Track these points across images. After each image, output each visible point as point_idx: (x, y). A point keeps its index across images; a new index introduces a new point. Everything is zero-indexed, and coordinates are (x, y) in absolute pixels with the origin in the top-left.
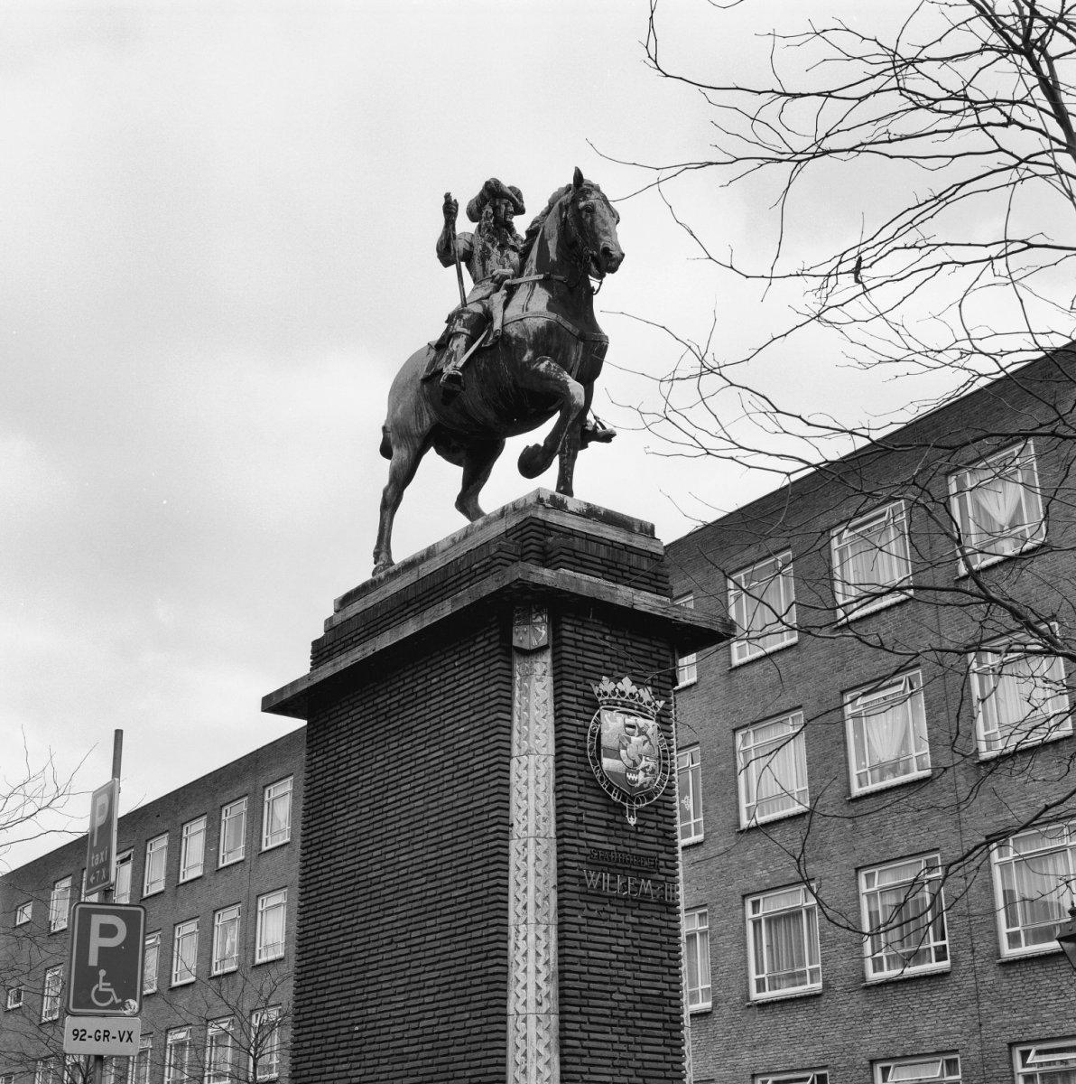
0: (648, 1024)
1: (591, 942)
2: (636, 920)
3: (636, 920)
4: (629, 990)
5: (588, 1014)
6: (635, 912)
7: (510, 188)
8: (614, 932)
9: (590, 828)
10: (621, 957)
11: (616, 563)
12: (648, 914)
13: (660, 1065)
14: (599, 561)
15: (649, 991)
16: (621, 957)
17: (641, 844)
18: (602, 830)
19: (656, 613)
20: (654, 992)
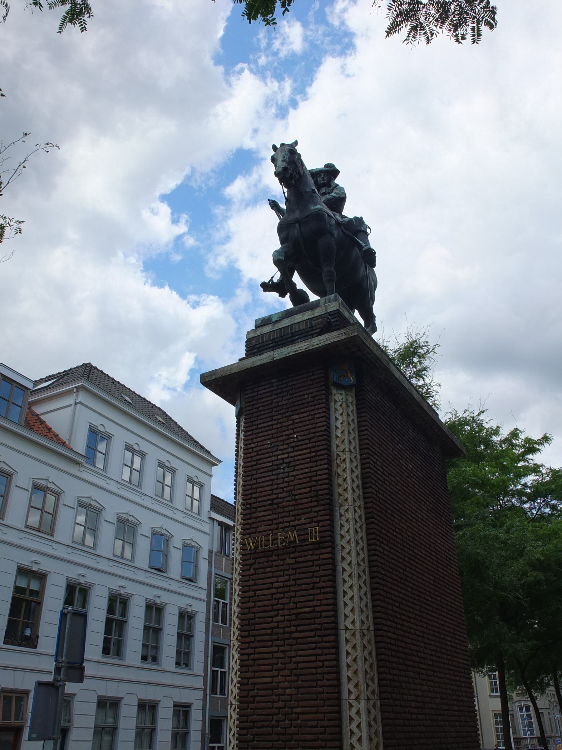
0: (302, 634)
1: (258, 585)
2: (293, 561)
3: (293, 561)
4: (286, 612)
5: (254, 636)
6: (292, 556)
7: (325, 167)
8: (275, 574)
10: (280, 590)
11: (282, 337)
12: (302, 554)
13: (312, 664)
14: (270, 342)
15: (303, 610)
16: (280, 590)
18: (267, 508)
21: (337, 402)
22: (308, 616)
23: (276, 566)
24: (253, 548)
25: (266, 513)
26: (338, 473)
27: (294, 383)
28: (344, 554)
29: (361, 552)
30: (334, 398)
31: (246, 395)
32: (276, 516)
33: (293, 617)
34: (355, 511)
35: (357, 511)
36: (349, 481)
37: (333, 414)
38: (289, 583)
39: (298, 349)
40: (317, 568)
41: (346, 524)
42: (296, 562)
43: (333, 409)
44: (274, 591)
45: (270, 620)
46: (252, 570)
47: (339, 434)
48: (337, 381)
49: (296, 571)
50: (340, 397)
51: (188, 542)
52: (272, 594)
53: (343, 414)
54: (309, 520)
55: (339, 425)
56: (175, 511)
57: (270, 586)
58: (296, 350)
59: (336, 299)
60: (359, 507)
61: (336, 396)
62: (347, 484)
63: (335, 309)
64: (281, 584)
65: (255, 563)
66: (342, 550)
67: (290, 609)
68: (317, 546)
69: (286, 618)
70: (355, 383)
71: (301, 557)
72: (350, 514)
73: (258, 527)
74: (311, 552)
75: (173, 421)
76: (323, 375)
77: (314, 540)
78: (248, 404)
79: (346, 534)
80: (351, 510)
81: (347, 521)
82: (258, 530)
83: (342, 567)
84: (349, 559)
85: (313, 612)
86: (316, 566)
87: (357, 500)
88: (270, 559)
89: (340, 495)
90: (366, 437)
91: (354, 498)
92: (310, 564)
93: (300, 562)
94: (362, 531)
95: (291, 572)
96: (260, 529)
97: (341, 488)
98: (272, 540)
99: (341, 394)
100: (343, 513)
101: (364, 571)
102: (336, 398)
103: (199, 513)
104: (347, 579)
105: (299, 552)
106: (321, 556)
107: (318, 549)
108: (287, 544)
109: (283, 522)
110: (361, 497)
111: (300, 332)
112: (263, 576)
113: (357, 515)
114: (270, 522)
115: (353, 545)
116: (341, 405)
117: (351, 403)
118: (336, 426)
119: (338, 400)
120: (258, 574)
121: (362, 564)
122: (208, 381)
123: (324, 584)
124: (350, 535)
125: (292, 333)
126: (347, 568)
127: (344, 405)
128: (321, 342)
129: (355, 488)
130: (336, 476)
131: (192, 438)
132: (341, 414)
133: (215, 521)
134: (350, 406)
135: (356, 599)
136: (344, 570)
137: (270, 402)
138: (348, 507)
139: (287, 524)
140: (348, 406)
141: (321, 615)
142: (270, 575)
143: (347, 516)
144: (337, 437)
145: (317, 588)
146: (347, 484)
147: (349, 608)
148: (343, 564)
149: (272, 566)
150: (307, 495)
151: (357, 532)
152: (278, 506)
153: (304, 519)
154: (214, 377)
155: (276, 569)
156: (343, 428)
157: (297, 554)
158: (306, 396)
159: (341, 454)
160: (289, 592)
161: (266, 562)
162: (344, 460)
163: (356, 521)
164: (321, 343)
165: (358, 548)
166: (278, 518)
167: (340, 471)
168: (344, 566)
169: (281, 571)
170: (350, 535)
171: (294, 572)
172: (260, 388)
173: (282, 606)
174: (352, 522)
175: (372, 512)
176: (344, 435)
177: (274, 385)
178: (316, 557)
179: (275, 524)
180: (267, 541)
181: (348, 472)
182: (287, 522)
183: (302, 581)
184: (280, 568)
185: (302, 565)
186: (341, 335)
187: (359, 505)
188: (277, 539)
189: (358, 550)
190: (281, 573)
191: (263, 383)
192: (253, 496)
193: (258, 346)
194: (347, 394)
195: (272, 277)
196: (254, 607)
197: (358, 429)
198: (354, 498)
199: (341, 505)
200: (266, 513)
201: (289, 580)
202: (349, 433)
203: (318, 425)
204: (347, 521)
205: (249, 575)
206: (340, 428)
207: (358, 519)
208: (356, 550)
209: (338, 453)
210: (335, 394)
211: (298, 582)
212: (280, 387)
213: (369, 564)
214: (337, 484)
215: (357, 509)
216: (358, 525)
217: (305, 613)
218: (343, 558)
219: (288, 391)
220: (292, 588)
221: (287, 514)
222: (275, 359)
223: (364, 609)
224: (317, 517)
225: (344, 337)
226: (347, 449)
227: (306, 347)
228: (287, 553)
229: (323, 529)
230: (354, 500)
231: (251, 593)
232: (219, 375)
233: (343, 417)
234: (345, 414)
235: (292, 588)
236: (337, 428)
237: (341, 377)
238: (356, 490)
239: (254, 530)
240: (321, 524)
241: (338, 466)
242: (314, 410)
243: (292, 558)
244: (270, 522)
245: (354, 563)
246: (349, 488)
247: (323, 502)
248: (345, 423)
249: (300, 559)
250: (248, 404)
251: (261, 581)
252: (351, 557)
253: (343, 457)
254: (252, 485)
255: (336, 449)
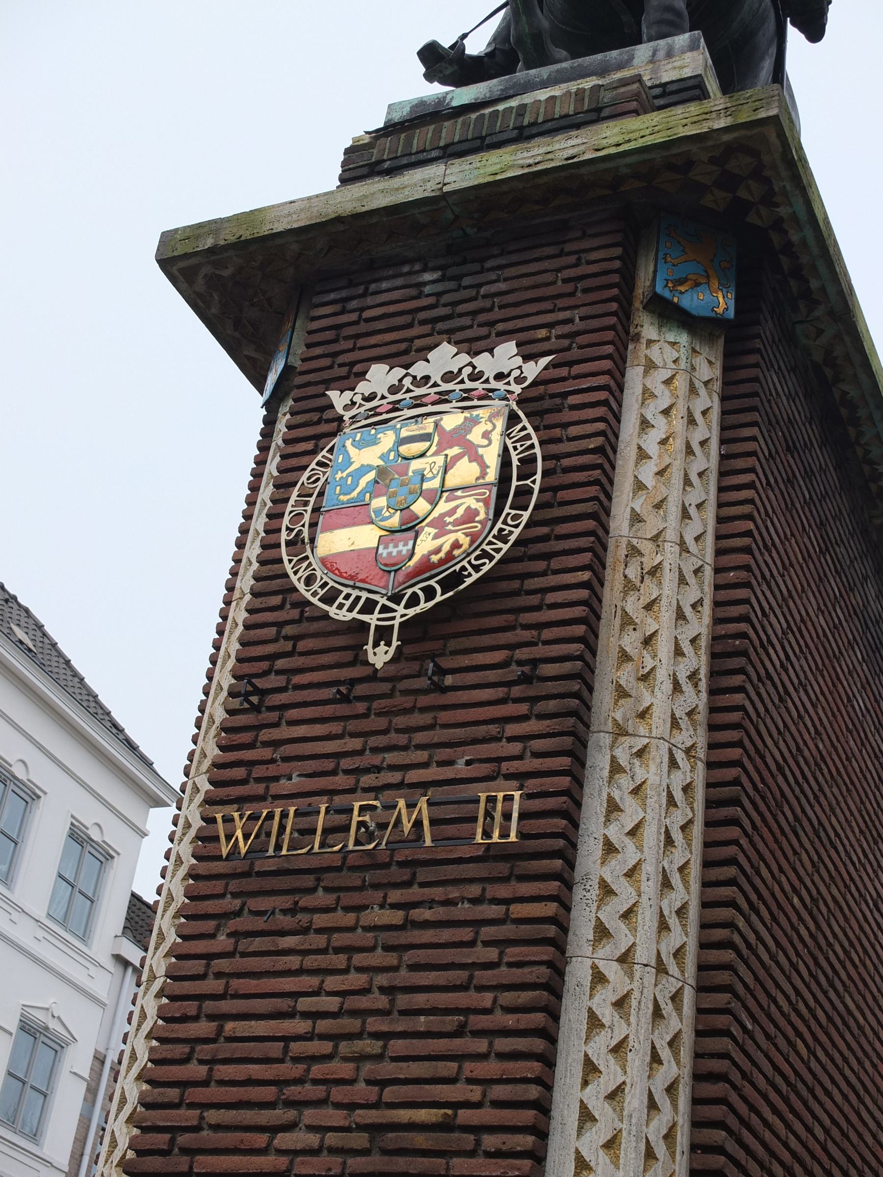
1: (236, 996)
2: (397, 917)
3: (397, 917)
4: (335, 1117)
6: (395, 896)
8: (311, 961)
9: (293, 714)
10: (323, 1025)
11: (483, 138)
12: (437, 893)
15: (405, 1115)
16: (323, 1025)
17: (445, 717)
19: (510, 174)
20: (423, 1115)
21: (655, 367)
22: (420, 1140)
23: (320, 931)
24: (243, 849)
25: (318, 730)
26: (625, 613)
27: (502, 286)
28: (610, 915)
29: (673, 921)
30: (648, 352)
31: (314, 319)
32: (355, 744)
33: (360, 1140)
34: (673, 764)
35: (679, 760)
36: (664, 647)
37: (636, 406)
38: (363, 1002)
39: (539, 159)
40: (492, 954)
41: (630, 804)
42: (409, 924)
43: (639, 390)
44: (300, 1026)
45: (261, 1139)
46: (222, 937)
47: (647, 476)
48: (667, 294)
49: (400, 958)
50: (670, 354)
51: (41, 1016)
52: (286, 1039)
53: (674, 412)
54: (484, 769)
55: (651, 446)
56: (15, 916)
57: (283, 1004)
58: (531, 161)
59: (693, 47)
60: (689, 751)
61: (656, 348)
62: (654, 656)
63: (687, 73)
64: (331, 1003)
65: (238, 913)
66: (601, 901)
67: (352, 1107)
68: (503, 868)
69: (332, 1139)
70: (731, 314)
71: (431, 903)
72: (653, 768)
73: (276, 779)
74: (475, 890)
75: (60, 654)
76: (617, 264)
77: (496, 838)
78: (318, 351)
79: (627, 840)
80: (659, 754)
81: (636, 791)
82: (275, 788)
83: (594, 967)
84: (623, 938)
85: (445, 1126)
86: (486, 944)
87: (683, 726)
88: (305, 901)
89: (622, 693)
90: (747, 509)
91: (673, 715)
92: (466, 934)
93: (426, 924)
94: (689, 845)
95: (379, 958)
96: (284, 786)
97: (629, 667)
98: (325, 831)
99: (673, 344)
100: (623, 761)
101: (676, 997)
102: (654, 353)
103: (85, 937)
104: (606, 1014)
105: (422, 885)
106: (512, 907)
107: (505, 880)
108: (383, 846)
109: (378, 769)
110: (702, 717)
111: (549, 125)
112: (266, 963)
113: (678, 780)
114: (329, 765)
115: (650, 887)
116: (668, 382)
117: (706, 383)
118: (640, 448)
119: (658, 361)
120: (244, 955)
121: (673, 969)
122: (186, 256)
123: (510, 1021)
124: (640, 848)
125: (521, 128)
126: (612, 970)
127: (681, 383)
128: (632, 136)
129: (682, 678)
130: (618, 622)
131: (108, 714)
132: (666, 412)
133: (130, 970)
134: (702, 391)
135: (635, 1101)
136: (599, 978)
137: (403, 346)
138: (647, 740)
139: (394, 777)
140: (693, 390)
141: (478, 1143)
142: (294, 962)
143: (640, 774)
144: (639, 486)
145: (478, 1033)
146: (654, 656)
147: (598, 1134)
148: (601, 953)
149: (304, 931)
150: (492, 676)
151: (669, 841)
152: (369, 709)
153: (468, 763)
154: (209, 242)
155: (320, 941)
156: (667, 460)
157: (415, 893)
158: (542, 333)
159: (646, 547)
160: (359, 1036)
161: (284, 912)
162: (655, 571)
163: (671, 802)
164: (629, 141)
165: (665, 904)
166: (360, 753)
167: (633, 606)
168: (601, 964)
169: (338, 950)
170: (640, 848)
171: (391, 959)
172: (370, 301)
173: (319, 1092)
174: (656, 801)
175: (736, 782)
176: (667, 484)
177: (427, 289)
178: (494, 911)
179: (347, 772)
180: (302, 832)
181: (667, 615)
182: (393, 768)
183: (421, 1000)
184: (339, 939)
185: (428, 936)
186: (714, 115)
187: (689, 744)
188: (346, 828)
189: (666, 913)
190: (339, 961)
191: (384, 285)
192: (280, 664)
193: (386, 165)
194: (694, 350)
195: (465, 36)
196: (205, 1083)
197: (719, 481)
198: (673, 715)
199: (621, 732)
200: (318, 730)
201: (365, 991)
202: (687, 482)
203: (573, 431)
204: (636, 791)
205: (209, 957)
206: (655, 457)
207: (678, 795)
208: (655, 909)
209: (634, 541)
210: (650, 342)
211: (403, 1001)
212: (445, 299)
213: (698, 979)
214: (614, 653)
215: (680, 756)
216: (678, 818)
217: (412, 1127)
218: (602, 932)
219: (474, 313)
220: (375, 1024)
221: (402, 739)
222: (446, 189)
223: (661, 1150)
224: (520, 757)
225: (721, 123)
226: (671, 535)
227: (570, 152)
228: (376, 886)
229: (537, 805)
230: (675, 723)
231: (204, 1028)
232: (228, 236)
233: (669, 423)
234: (680, 412)
235: (375, 1024)
236: (643, 455)
237: (681, 282)
238: (687, 687)
239: (260, 789)
240: (533, 785)
241: (629, 587)
242: (563, 379)
243: (394, 906)
244: (329, 765)
245: (643, 954)
246: (662, 675)
247: (552, 705)
248: (677, 444)
249: (425, 914)
250: (318, 351)
251: (254, 982)
252: (634, 930)
253: (649, 562)
254: (280, 625)
255: (632, 526)
